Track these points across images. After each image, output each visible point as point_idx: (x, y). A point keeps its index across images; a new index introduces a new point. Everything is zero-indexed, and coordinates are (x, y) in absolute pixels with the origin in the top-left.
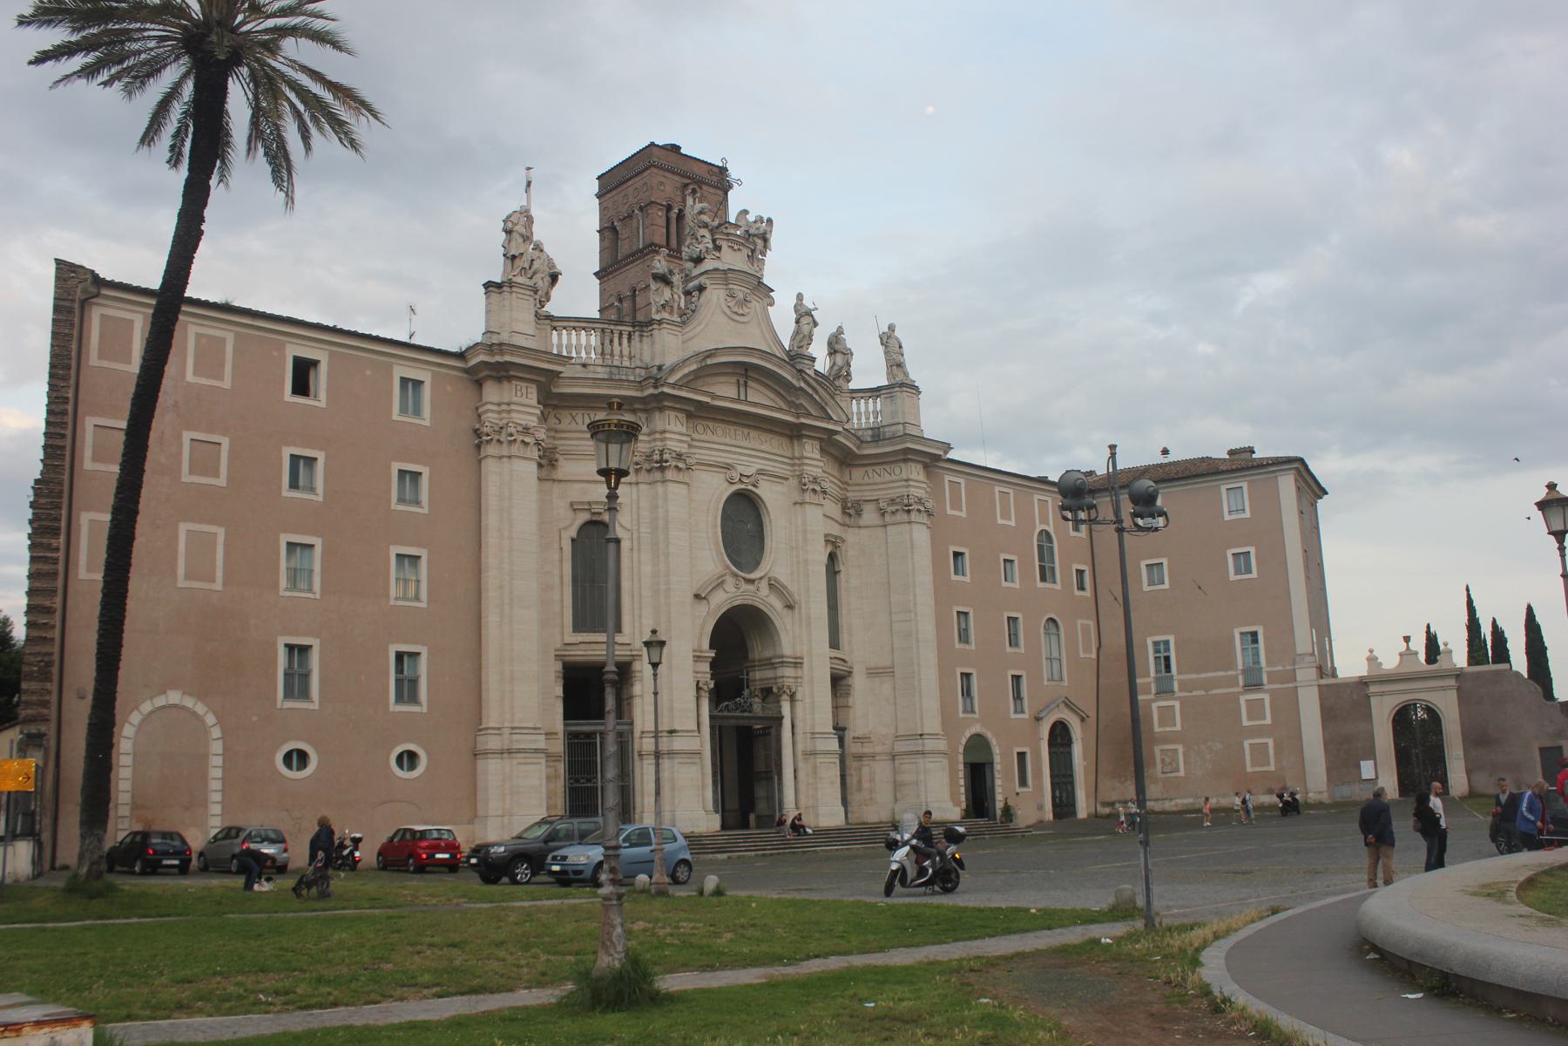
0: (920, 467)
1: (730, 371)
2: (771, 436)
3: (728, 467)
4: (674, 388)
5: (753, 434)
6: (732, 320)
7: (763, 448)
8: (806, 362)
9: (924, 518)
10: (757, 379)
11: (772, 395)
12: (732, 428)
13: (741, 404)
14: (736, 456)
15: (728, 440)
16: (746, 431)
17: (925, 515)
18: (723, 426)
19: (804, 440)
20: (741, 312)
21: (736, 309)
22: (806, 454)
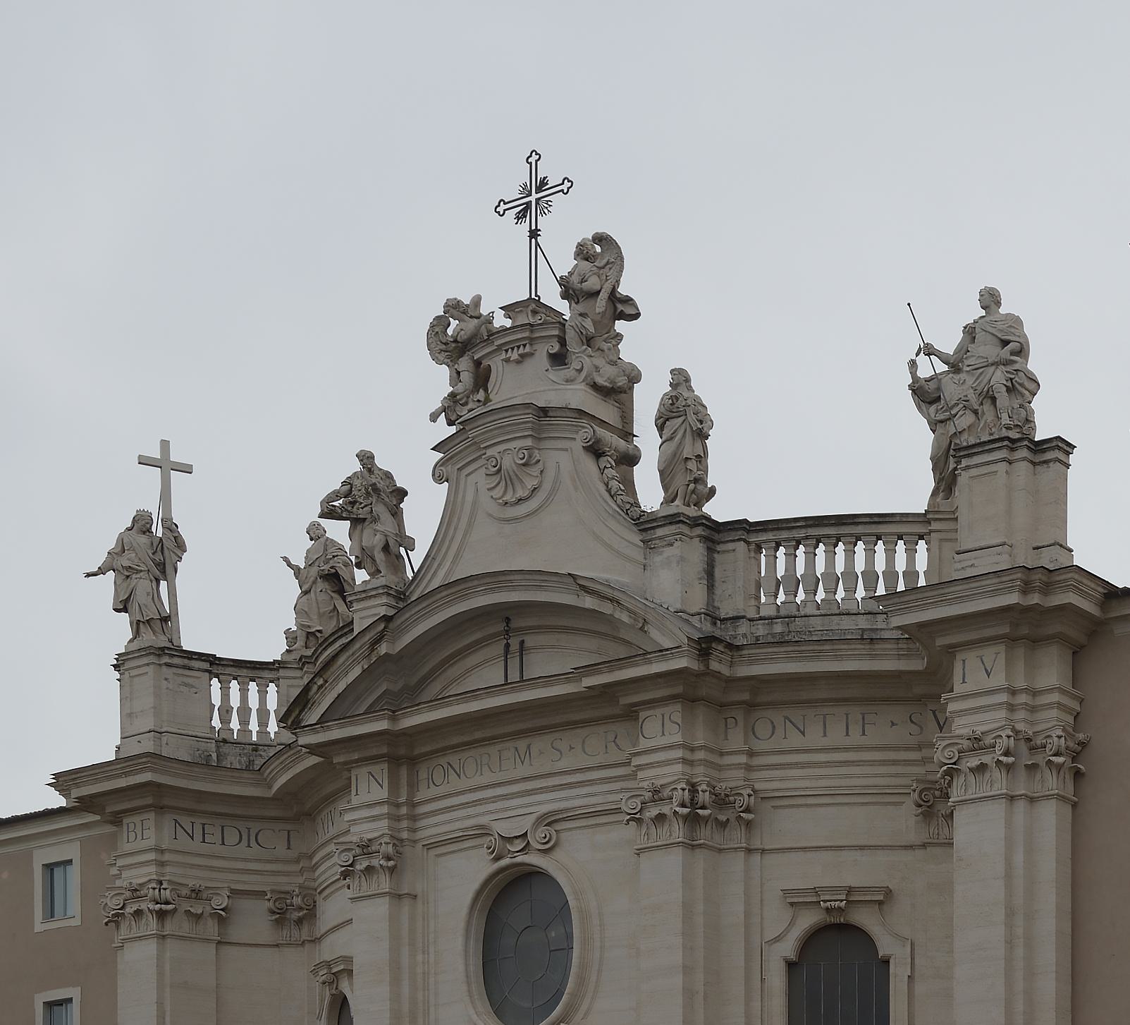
0: (995, 656)
1: (478, 635)
2: (582, 732)
3: (484, 832)
4: (316, 732)
5: (538, 744)
6: (508, 520)
7: (564, 764)
8: (660, 532)
9: (998, 783)
10: (539, 627)
11: (592, 643)
12: (493, 750)
13: (514, 690)
14: (499, 805)
15: (488, 778)
16: (522, 744)
17: (997, 773)
18: (472, 752)
19: (642, 715)
20: (521, 493)
21: (507, 498)
22: (644, 744)
